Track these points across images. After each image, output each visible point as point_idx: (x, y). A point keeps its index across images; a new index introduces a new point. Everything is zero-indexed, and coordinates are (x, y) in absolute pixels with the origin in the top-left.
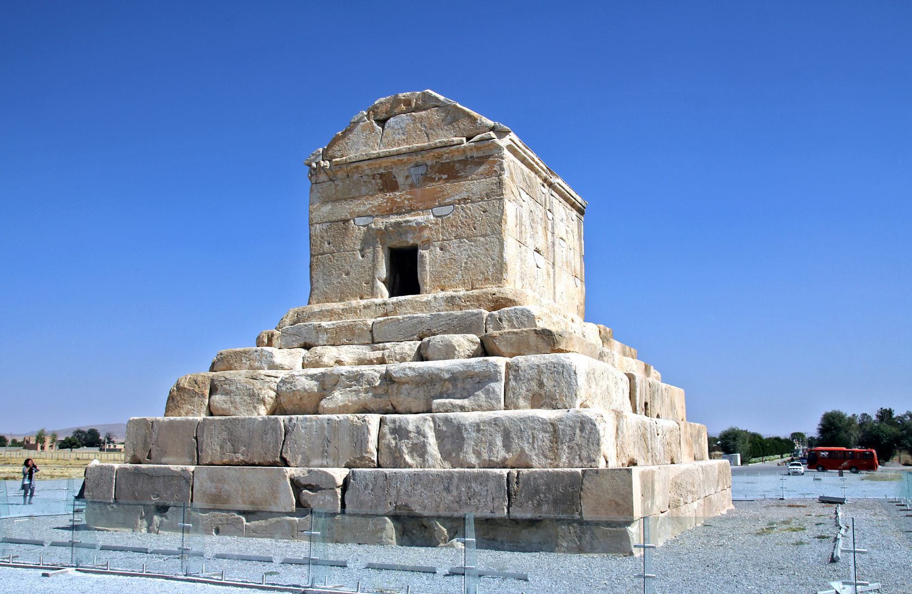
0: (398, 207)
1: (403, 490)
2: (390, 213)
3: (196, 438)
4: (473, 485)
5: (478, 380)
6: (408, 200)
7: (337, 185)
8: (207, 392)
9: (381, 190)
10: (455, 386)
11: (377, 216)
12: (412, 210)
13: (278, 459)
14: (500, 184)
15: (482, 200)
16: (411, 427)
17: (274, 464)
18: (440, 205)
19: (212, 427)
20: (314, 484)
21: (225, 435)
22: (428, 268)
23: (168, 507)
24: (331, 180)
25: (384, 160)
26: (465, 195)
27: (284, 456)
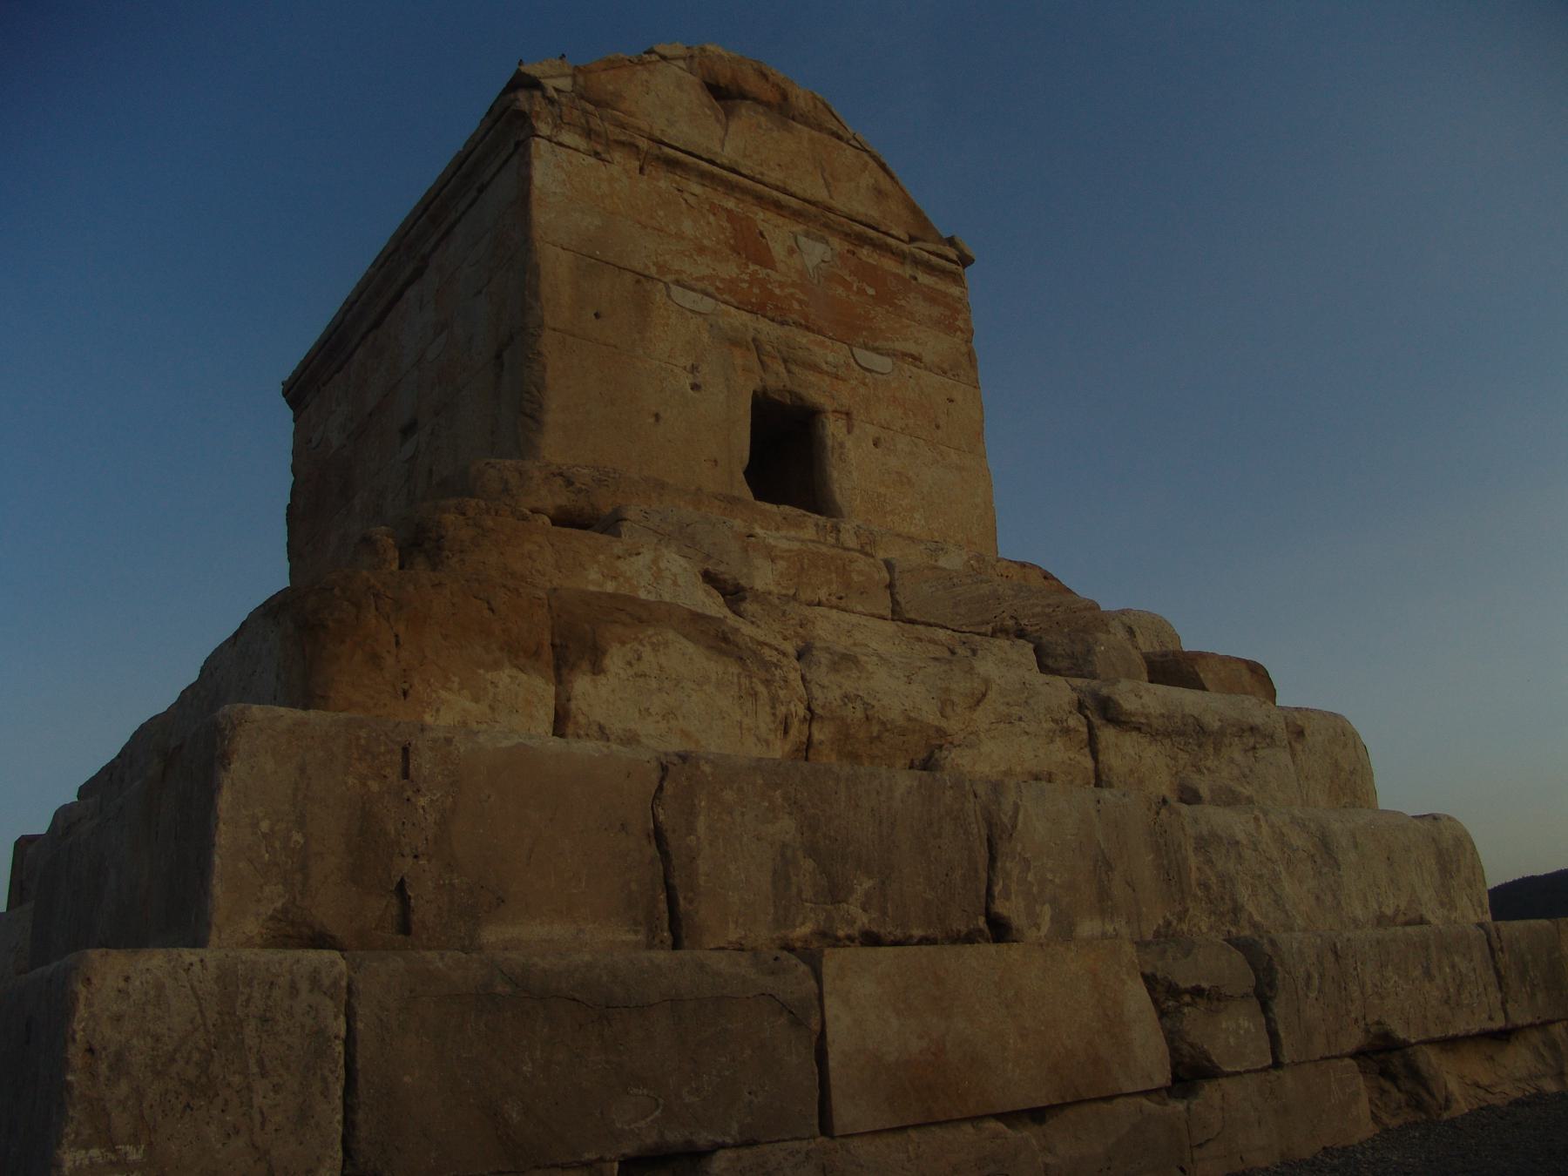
0: (776, 307)
1: (1369, 984)
2: (757, 310)
3: (658, 836)
4: (1457, 959)
5: (1252, 741)
6: (800, 302)
8: (547, 654)
9: (735, 250)
10: (1217, 750)
11: (726, 303)
12: (808, 328)
13: (981, 922)
15: (945, 373)
16: (1241, 837)
18: (866, 347)
19: (729, 795)
20: (1205, 985)
21: (786, 827)
22: (855, 474)
26: (911, 347)
27: (1001, 907)
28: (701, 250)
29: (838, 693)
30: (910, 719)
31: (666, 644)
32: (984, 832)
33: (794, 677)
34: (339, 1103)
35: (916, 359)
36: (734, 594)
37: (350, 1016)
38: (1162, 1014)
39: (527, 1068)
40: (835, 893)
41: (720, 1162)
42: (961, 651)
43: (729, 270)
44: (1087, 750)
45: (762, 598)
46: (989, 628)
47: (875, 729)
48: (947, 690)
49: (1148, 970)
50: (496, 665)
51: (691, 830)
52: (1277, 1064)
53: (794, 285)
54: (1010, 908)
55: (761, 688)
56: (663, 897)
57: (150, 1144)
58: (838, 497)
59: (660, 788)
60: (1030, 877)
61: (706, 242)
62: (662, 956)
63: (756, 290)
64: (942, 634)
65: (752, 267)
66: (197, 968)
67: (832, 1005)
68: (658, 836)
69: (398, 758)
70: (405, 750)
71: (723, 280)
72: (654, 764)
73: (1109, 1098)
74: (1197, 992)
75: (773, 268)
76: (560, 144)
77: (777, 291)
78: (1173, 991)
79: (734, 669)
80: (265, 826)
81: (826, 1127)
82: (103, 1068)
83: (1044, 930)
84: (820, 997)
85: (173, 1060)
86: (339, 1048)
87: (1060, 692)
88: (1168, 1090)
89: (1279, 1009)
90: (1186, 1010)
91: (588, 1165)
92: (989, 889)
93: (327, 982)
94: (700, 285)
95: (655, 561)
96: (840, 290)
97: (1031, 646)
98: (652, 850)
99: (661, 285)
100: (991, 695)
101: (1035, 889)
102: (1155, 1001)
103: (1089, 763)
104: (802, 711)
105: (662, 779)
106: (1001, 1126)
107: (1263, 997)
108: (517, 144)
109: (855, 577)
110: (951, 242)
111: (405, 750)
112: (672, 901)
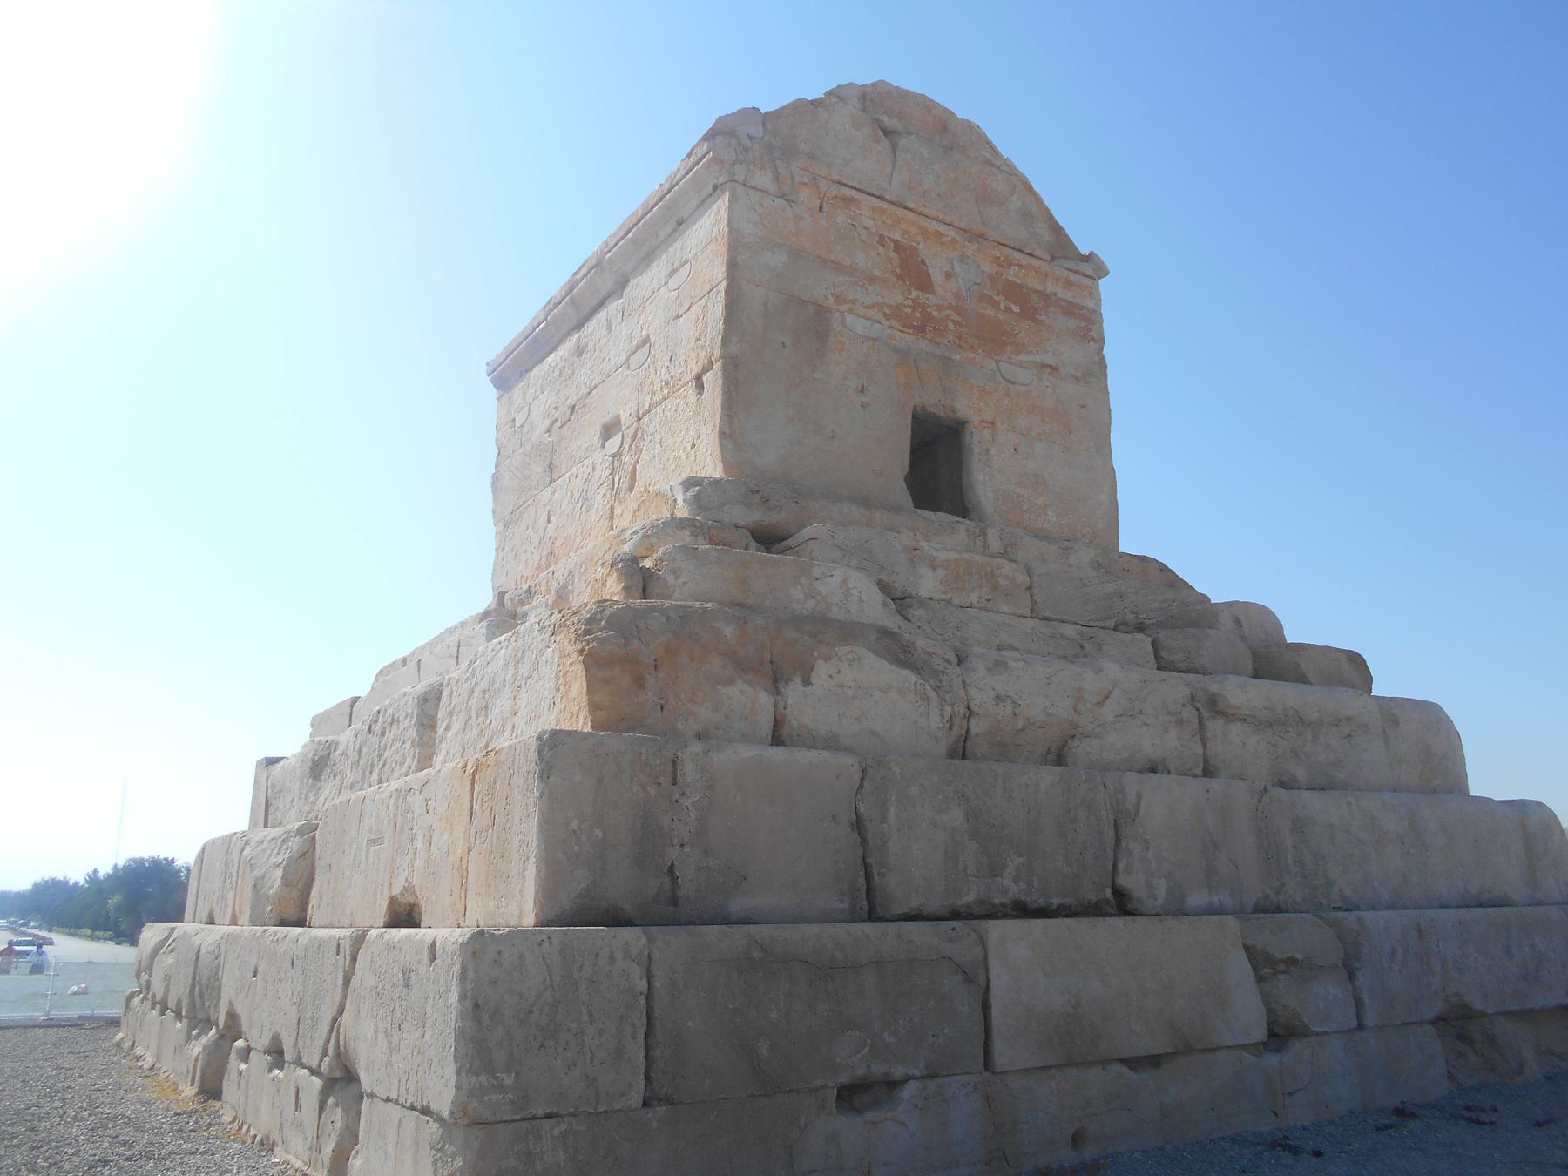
2: (920, 330)
3: (858, 825)
6: (955, 323)
7: (798, 218)
9: (899, 277)
13: (1108, 893)
14: (1103, 365)
15: (1078, 380)
17: (1094, 910)
20: (1299, 956)
21: (956, 815)
23: (892, 1085)
24: (782, 196)
25: (911, 215)
26: (1048, 359)
27: (1123, 881)
28: (872, 280)
29: (992, 694)
30: (1048, 715)
31: (859, 659)
32: (1112, 817)
33: (957, 682)
34: (642, 1042)
35: (1054, 369)
36: (901, 601)
37: (650, 978)
38: (1260, 979)
39: (773, 1016)
40: (994, 870)
41: (909, 1091)
42: (1088, 646)
43: (897, 297)
44: (1197, 738)
45: (924, 602)
46: (1112, 623)
47: (1020, 723)
48: (1080, 689)
49: (1249, 943)
50: (730, 682)
51: (884, 819)
52: (1361, 1027)
53: (950, 307)
54: (1131, 882)
55: (932, 694)
56: (862, 873)
57: (517, 1073)
58: (983, 499)
59: (861, 786)
60: (1150, 855)
61: (877, 273)
62: (869, 928)
63: (917, 314)
64: (1070, 630)
65: (915, 293)
66: (546, 944)
67: (995, 968)
68: (858, 825)
69: (669, 768)
70: (674, 762)
71: (889, 306)
72: (856, 767)
73: (1214, 1050)
74: (1291, 962)
75: (932, 292)
76: (754, 188)
77: (935, 314)
78: (1271, 961)
79: (912, 677)
80: (575, 824)
81: (988, 1064)
82: (486, 1018)
83: (1160, 900)
84: (986, 959)
85: (531, 1012)
86: (642, 1001)
87: (1175, 688)
88: (1264, 1044)
89: (1361, 978)
90: (1282, 977)
91: (817, 1090)
92: (1115, 865)
93: (634, 952)
94: (871, 313)
95: (845, 582)
96: (990, 312)
97: (1149, 640)
98: (855, 836)
99: (837, 315)
100: (1116, 692)
101: (1154, 866)
102: (1255, 969)
103: (1199, 749)
104: (963, 711)
105: (862, 779)
106: (1124, 1069)
107: (1349, 970)
108: (715, 188)
109: (1002, 582)
110: (1090, 258)
111: (674, 762)
112: (868, 877)
